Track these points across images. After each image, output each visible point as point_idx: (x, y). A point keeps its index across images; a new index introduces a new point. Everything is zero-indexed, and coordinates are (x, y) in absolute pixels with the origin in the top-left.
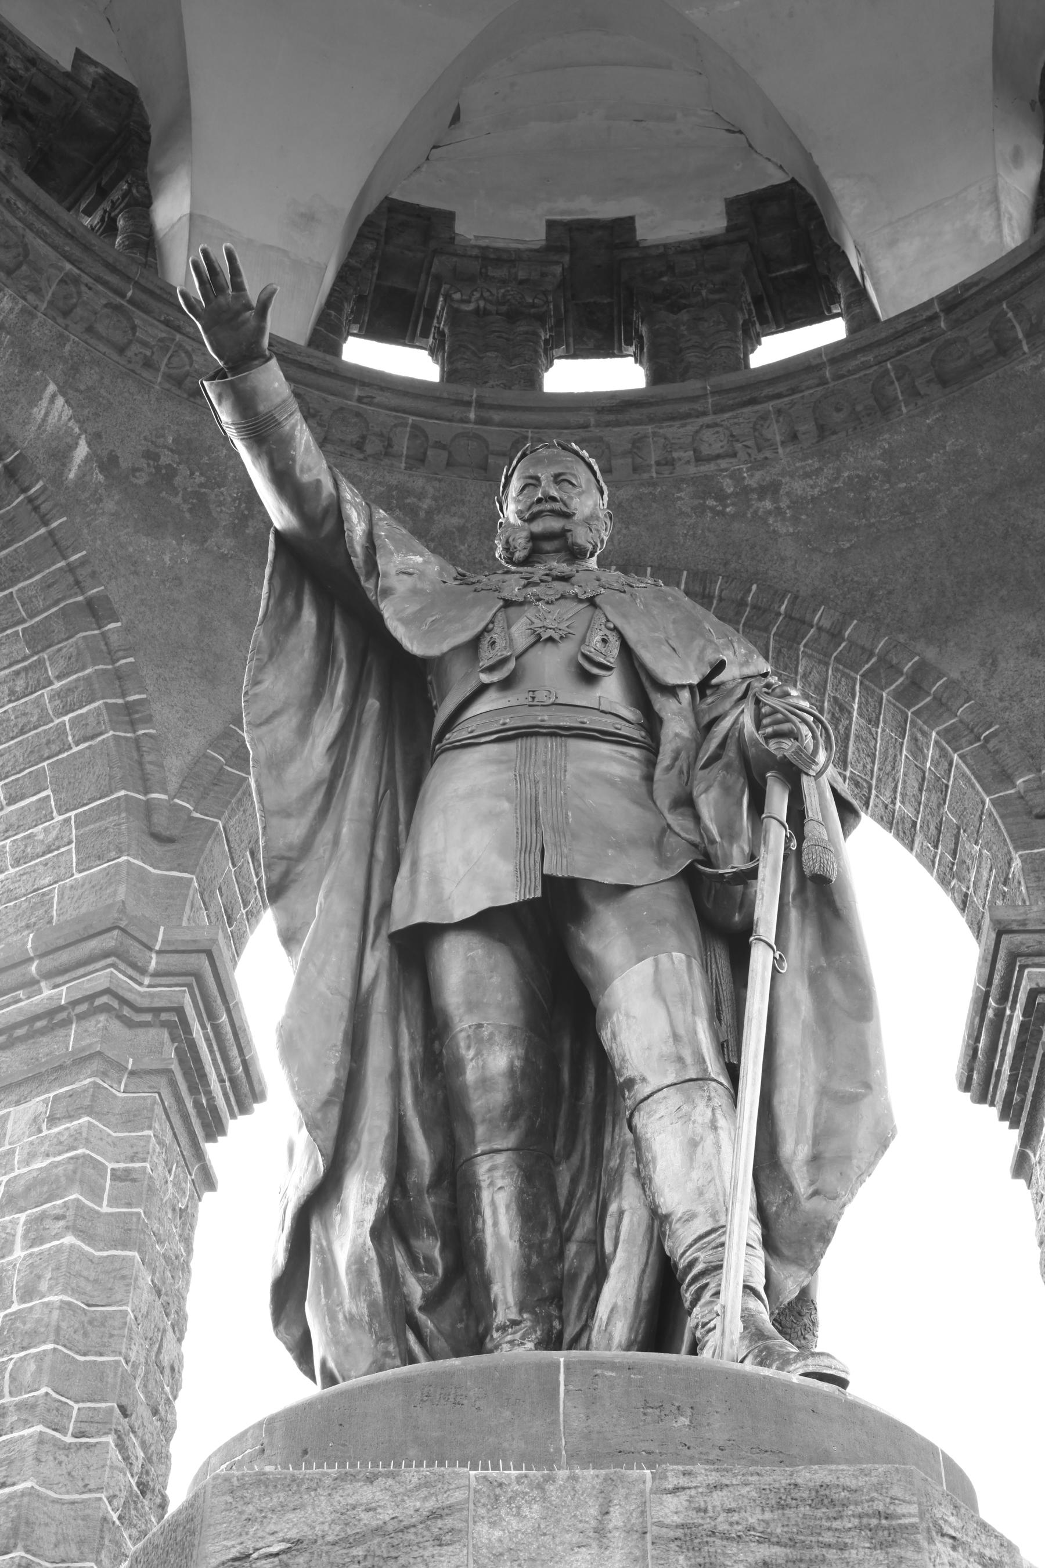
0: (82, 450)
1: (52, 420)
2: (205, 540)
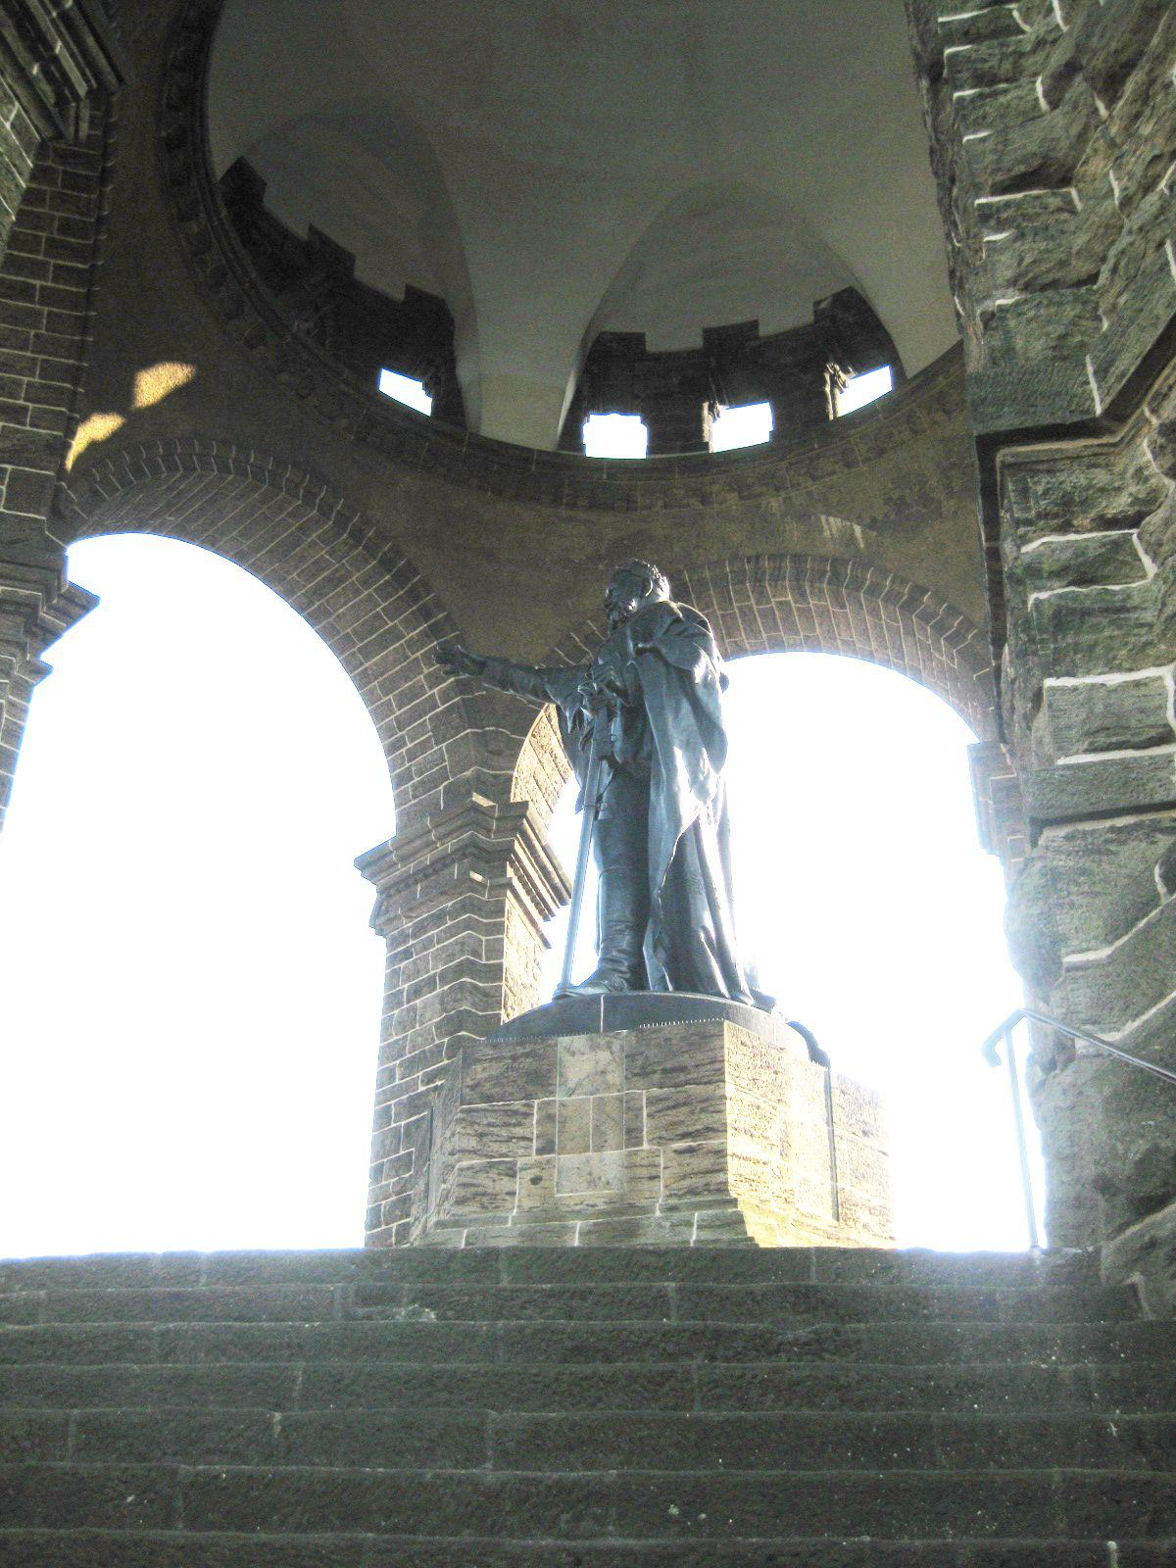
0: (858, 530)
1: (834, 531)
2: (941, 514)
